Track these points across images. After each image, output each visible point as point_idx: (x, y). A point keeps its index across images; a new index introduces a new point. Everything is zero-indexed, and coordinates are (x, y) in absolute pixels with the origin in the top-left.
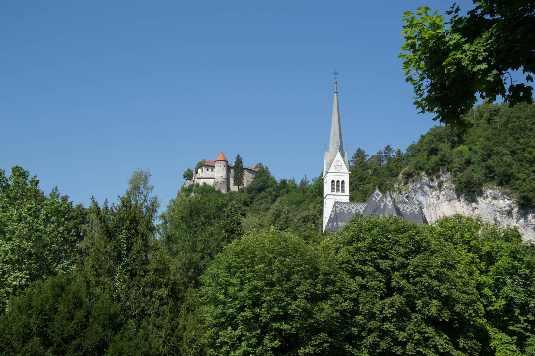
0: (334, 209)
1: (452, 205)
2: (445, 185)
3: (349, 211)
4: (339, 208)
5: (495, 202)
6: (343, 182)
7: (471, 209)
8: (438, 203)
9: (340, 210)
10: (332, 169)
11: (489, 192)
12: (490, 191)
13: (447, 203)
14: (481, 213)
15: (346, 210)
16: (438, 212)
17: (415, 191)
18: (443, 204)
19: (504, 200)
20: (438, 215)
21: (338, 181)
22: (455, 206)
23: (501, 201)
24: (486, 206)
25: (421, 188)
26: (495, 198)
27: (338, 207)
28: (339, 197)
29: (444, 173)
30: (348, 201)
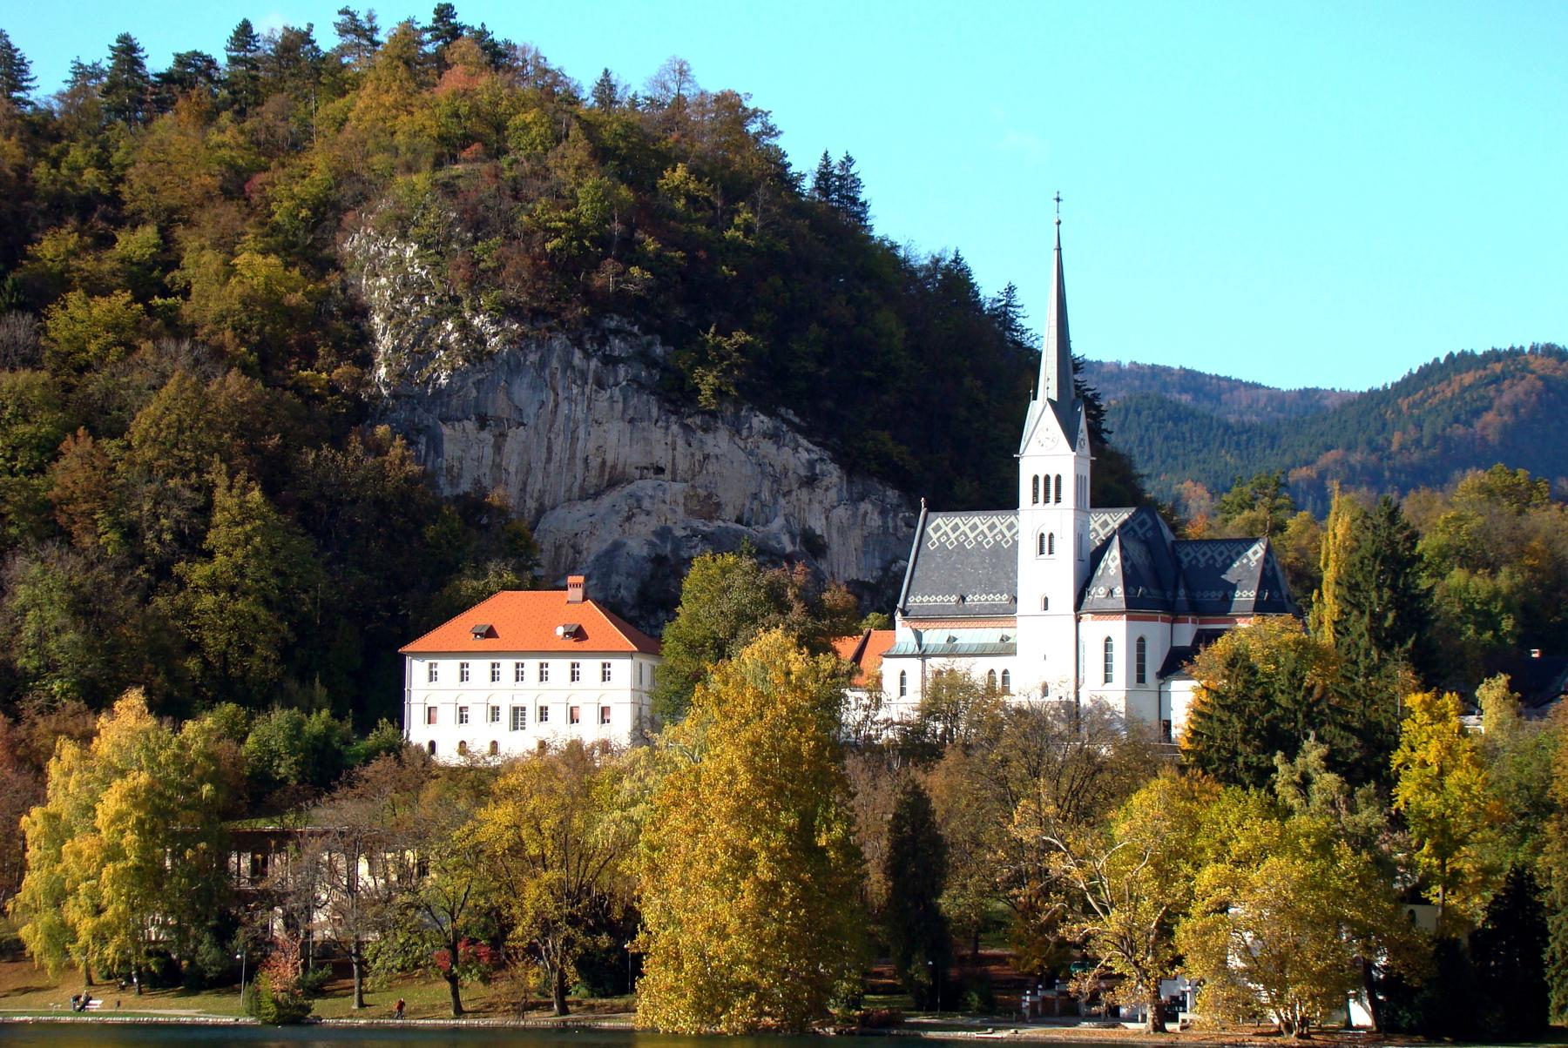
5: (767, 447)
7: (699, 456)
8: (586, 421)
11: (760, 421)
12: (762, 417)
13: (622, 425)
16: (580, 445)
18: (606, 426)
19: (795, 450)
20: (579, 455)
22: (647, 441)
23: (787, 451)
24: (742, 456)
25: (543, 364)
29: (616, 332)
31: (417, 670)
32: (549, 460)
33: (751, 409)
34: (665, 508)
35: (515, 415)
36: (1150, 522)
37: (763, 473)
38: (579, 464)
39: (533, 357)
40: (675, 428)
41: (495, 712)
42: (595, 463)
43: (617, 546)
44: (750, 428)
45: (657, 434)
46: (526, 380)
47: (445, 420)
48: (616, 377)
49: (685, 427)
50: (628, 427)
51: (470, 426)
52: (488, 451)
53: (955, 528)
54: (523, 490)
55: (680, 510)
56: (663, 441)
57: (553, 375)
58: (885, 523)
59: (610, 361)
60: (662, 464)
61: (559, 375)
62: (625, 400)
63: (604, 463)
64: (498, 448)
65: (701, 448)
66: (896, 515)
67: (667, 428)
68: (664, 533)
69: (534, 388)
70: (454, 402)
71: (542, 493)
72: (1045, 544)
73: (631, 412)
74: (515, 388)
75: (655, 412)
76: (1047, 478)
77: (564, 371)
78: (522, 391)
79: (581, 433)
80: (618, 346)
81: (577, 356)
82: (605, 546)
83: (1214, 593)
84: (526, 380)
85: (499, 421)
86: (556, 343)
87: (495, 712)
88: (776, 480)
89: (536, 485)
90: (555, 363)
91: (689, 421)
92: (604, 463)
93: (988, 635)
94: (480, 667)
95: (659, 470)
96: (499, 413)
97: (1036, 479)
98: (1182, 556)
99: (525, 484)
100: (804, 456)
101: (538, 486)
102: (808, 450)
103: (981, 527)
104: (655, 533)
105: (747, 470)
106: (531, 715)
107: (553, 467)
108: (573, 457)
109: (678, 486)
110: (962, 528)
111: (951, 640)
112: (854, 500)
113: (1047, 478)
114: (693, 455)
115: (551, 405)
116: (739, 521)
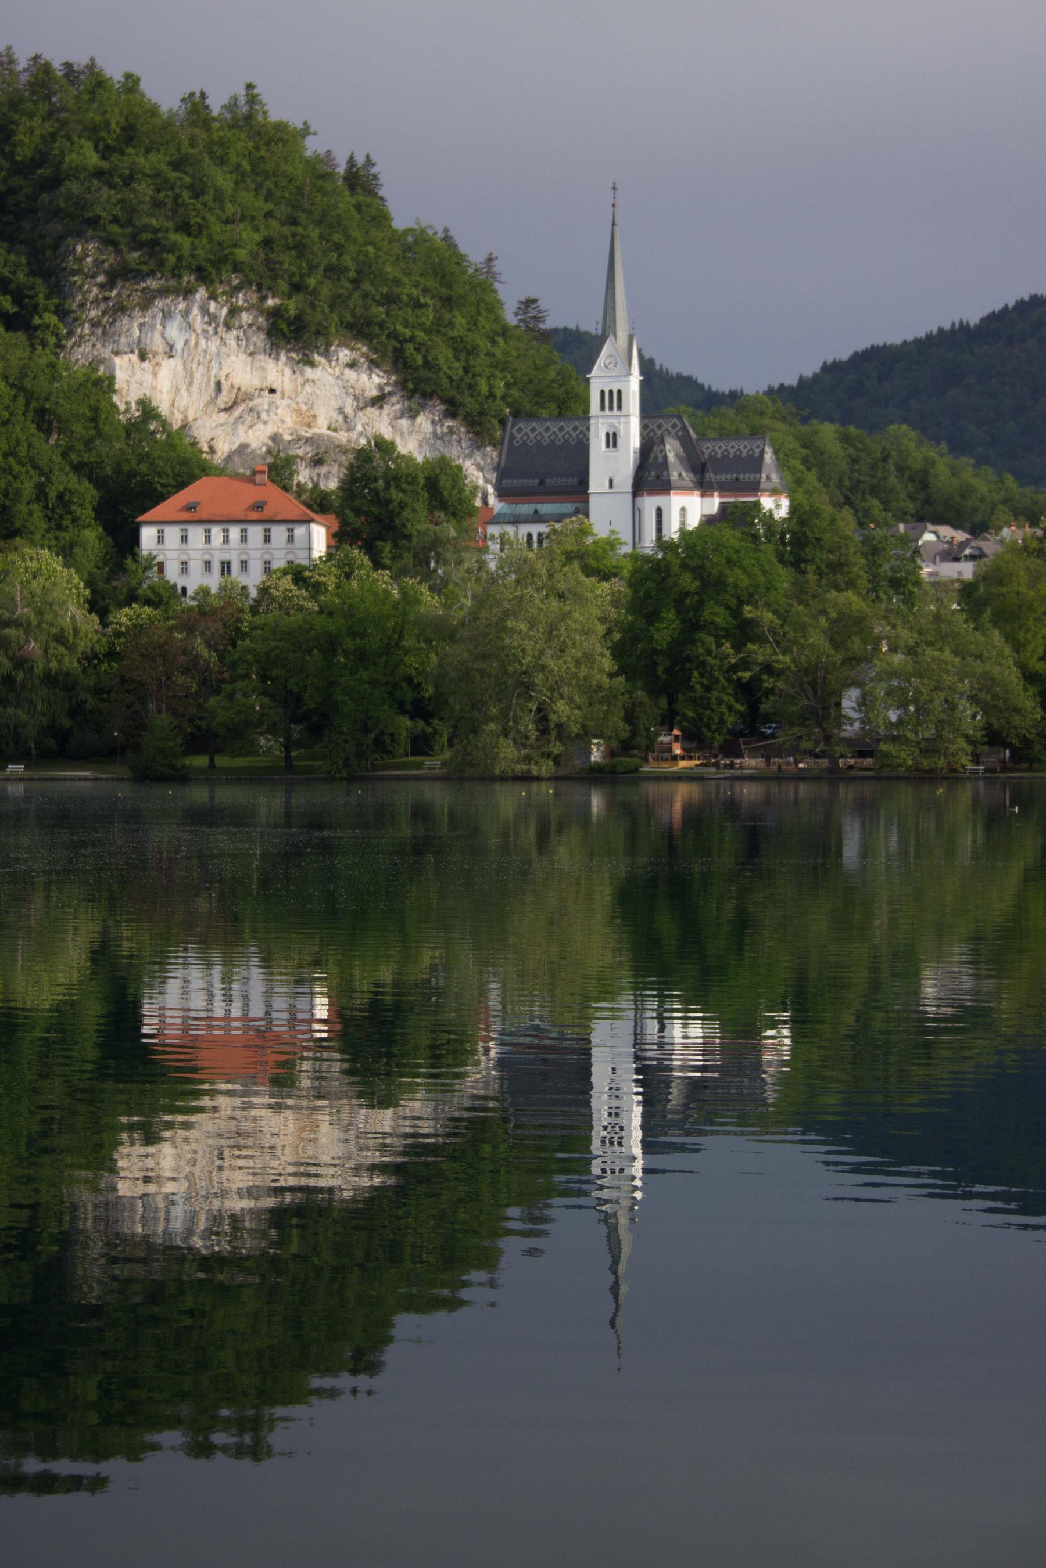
1: (257, 364)
5: (350, 374)
7: (300, 380)
8: (218, 354)
11: (345, 355)
12: (347, 352)
13: (242, 357)
14: (318, 391)
16: (214, 372)
17: (167, 315)
18: (233, 358)
22: (264, 369)
23: (364, 377)
25: (186, 313)
26: (352, 365)
28: (614, 421)
31: (148, 535)
32: (191, 384)
33: (338, 346)
35: (168, 350)
36: (680, 425)
37: (347, 393)
38: (213, 385)
39: (182, 306)
40: (283, 358)
41: (208, 565)
43: (243, 447)
45: (270, 365)
47: (117, 353)
48: (240, 321)
49: (288, 358)
50: (249, 359)
51: (134, 358)
52: (148, 378)
53: (533, 430)
54: (173, 405)
56: (277, 371)
57: (194, 320)
58: (435, 431)
59: (233, 312)
60: (274, 387)
62: (248, 340)
63: (232, 386)
64: (155, 375)
65: (302, 374)
66: (442, 425)
67: (277, 359)
68: (275, 438)
70: (123, 340)
71: (187, 408)
72: (612, 440)
73: (252, 348)
75: (268, 351)
76: (611, 392)
77: (203, 317)
78: (174, 331)
80: (240, 300)
82: (234, 447)
83: (729, 476)
85: (155, 354)
86: (198, 296)
87: (208, 565)
88: (356, 398)
89: (183, 400)
90: (195, 311)
92: (232, 386)
93: (567, 507)
94: (196, 533)
95: (272, 391)
96: (155, 348)
97: (602, 392)
98: (704, 449)
99: (174, 401)
100: (376, 380)
101: (185, 403)
102: (378, 375)
103: (553, 429)
105: (337, 391)
106: (235, 567)
107: (195, 388)
108: (209, 381)
109: (285, 402)
110: (567, 429)
111: (536, 512)
112: (412, 414)
113: (611, 392)
114: (296, 380)
115: (193, 343)
116: (329, 428)
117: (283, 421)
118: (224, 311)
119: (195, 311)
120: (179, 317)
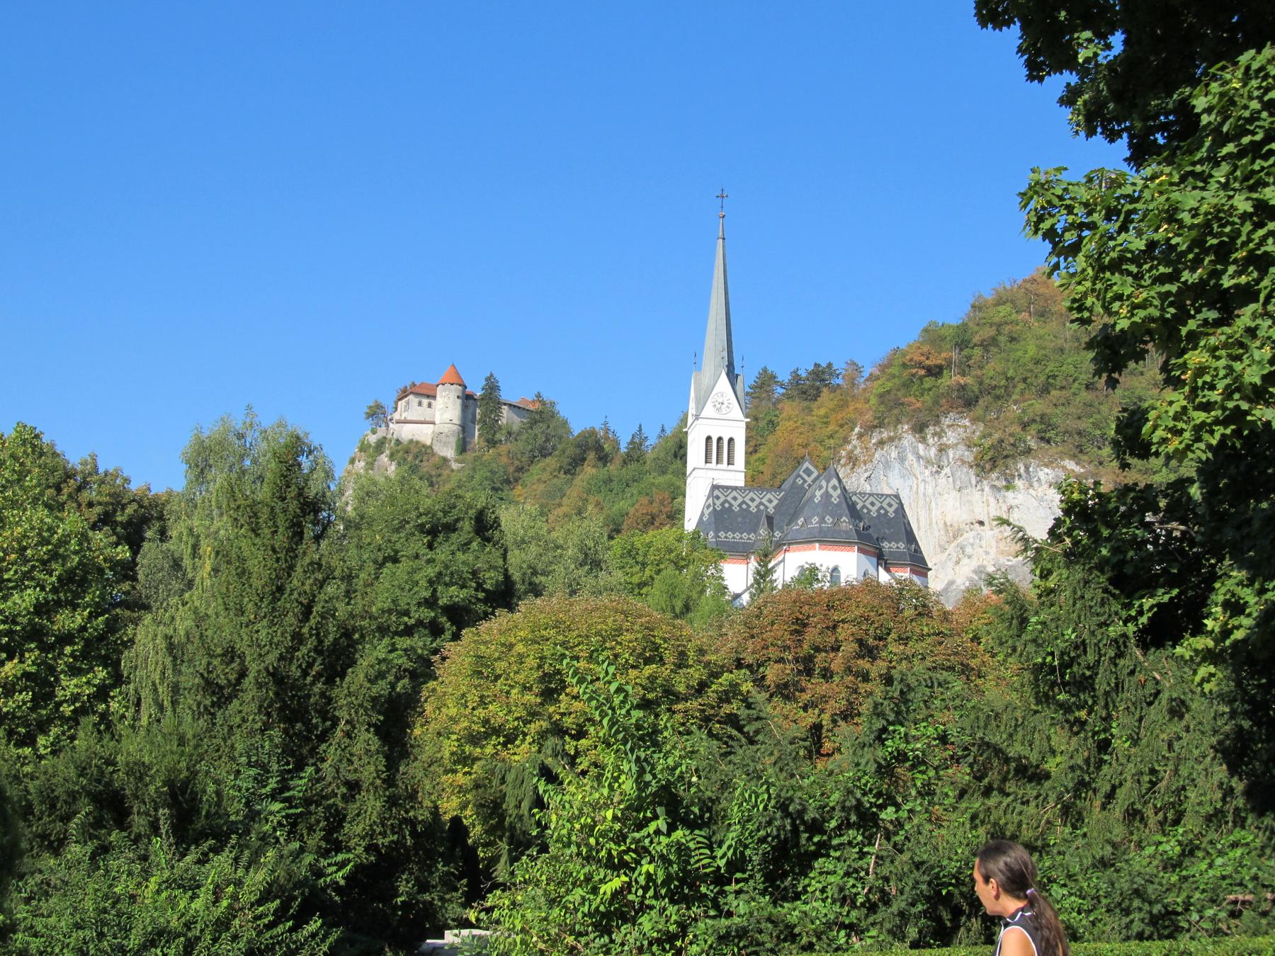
0: (710, 501)
2: (951, 453)
3: (744, 506)
4: (721, 500)
6: (731, 440)
9: (722, 504)
10: (709, 410)
12: (1046, 470)
13: (954, 493)
15: (735, 504)
17: (887, 465)
21: (720, 439)
22: (969, 501)
24: (1036, 504)
25: (902, 459)
27: (718, 498)
30: (742, 484)
34: (981, 550)
39: (894, 454)
40: (987, 489)
42: (941, 525)
43: (951, 583)
44: (1039, 480)
45: (977, 495)
46: (896, 471)
50: (958, 495)
55: (993, 551)
59: (942, 449)
61: (915, 465)
69: (903, 477)
74: (891, 480)
75: (974, 482)
79: (933, 505)
81: (921, 446)
84: (896, 471)
90: (910, 457)
91: (996, 483)
95: (981, 523)
104: (975, 572)
117: (987, 553)
118: (933, 452)
119: (910, 457)
120: (897, 465)
